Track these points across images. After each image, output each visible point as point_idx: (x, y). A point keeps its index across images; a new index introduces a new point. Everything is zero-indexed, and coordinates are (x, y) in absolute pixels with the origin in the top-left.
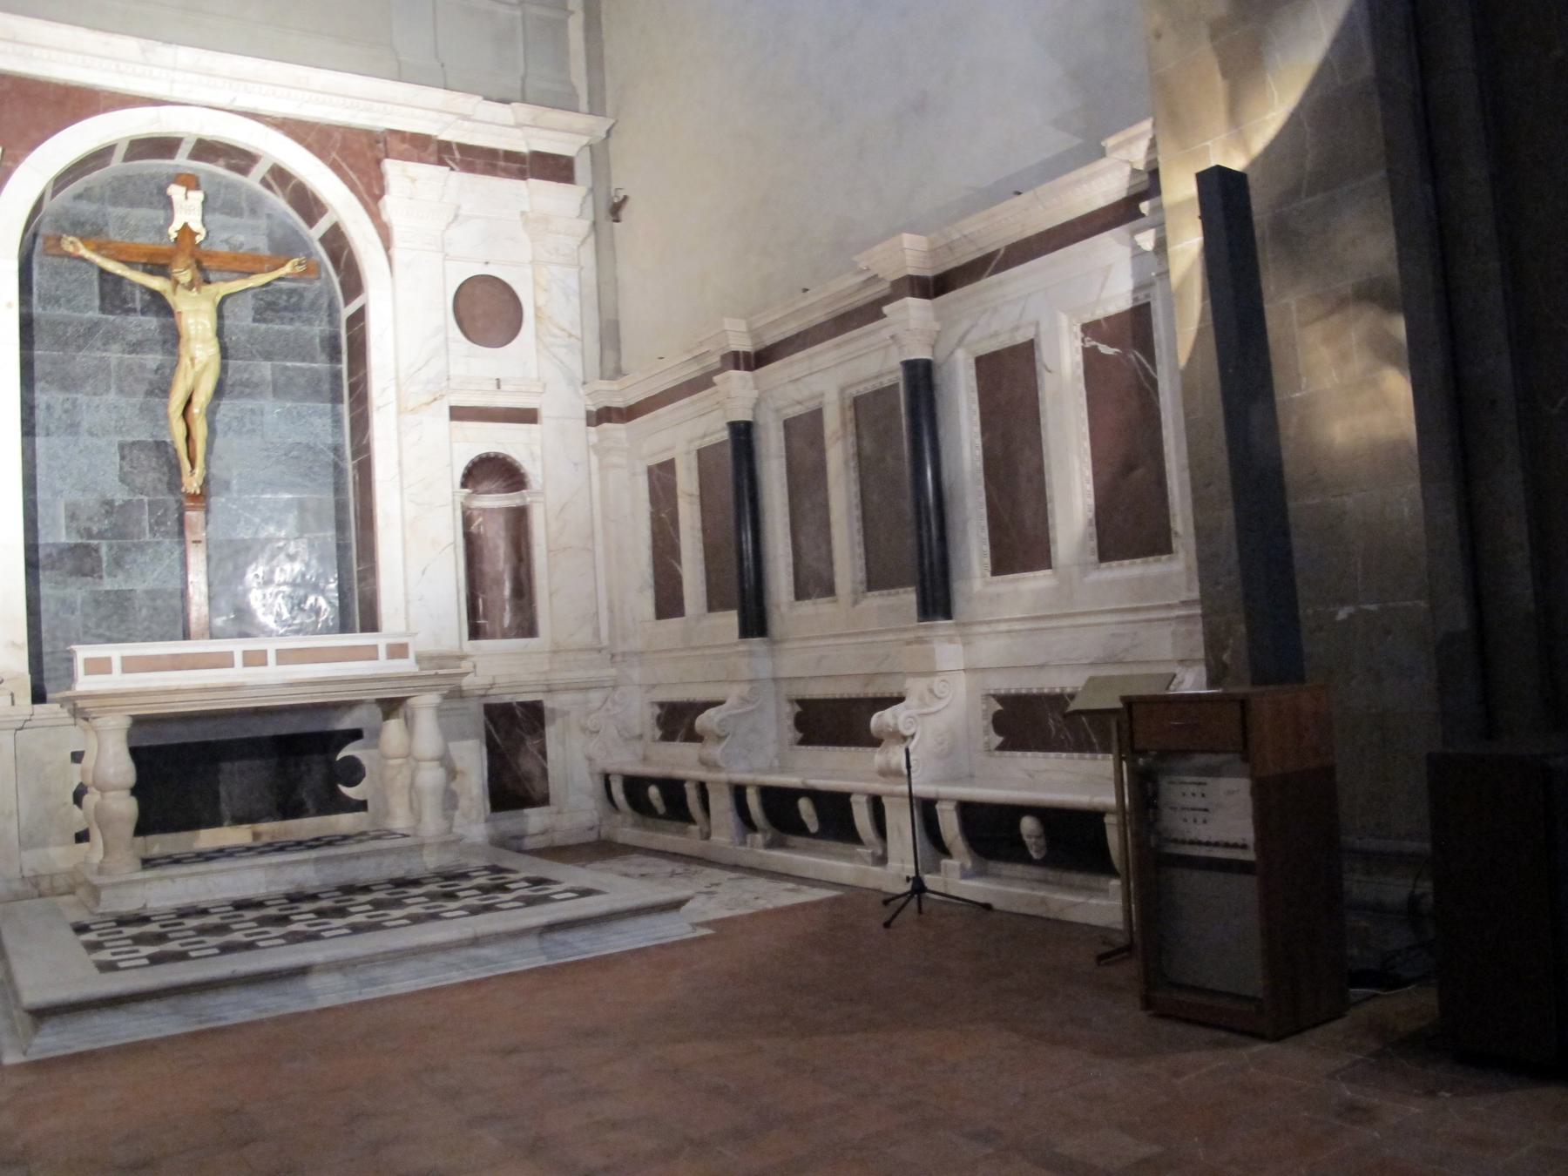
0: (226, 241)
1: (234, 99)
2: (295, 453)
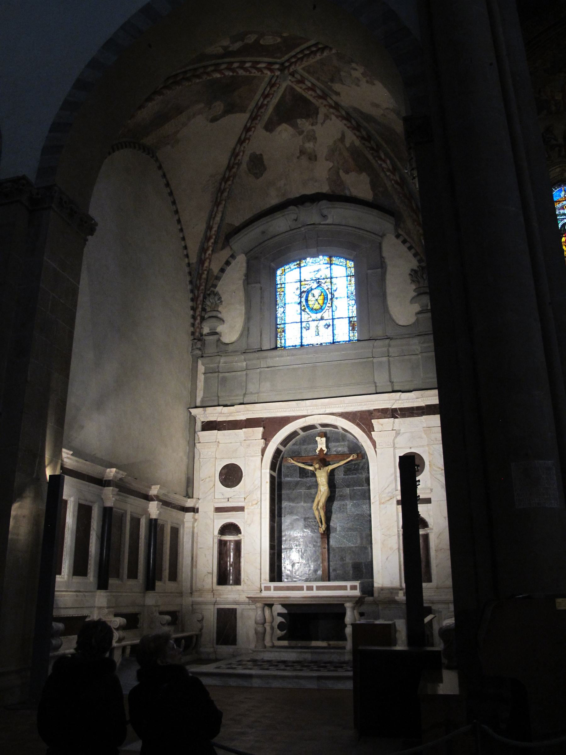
0: (335, 451)
1: (325, 411)
2: (357, 518)
